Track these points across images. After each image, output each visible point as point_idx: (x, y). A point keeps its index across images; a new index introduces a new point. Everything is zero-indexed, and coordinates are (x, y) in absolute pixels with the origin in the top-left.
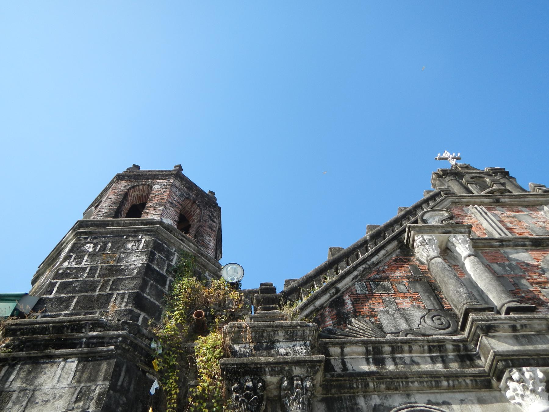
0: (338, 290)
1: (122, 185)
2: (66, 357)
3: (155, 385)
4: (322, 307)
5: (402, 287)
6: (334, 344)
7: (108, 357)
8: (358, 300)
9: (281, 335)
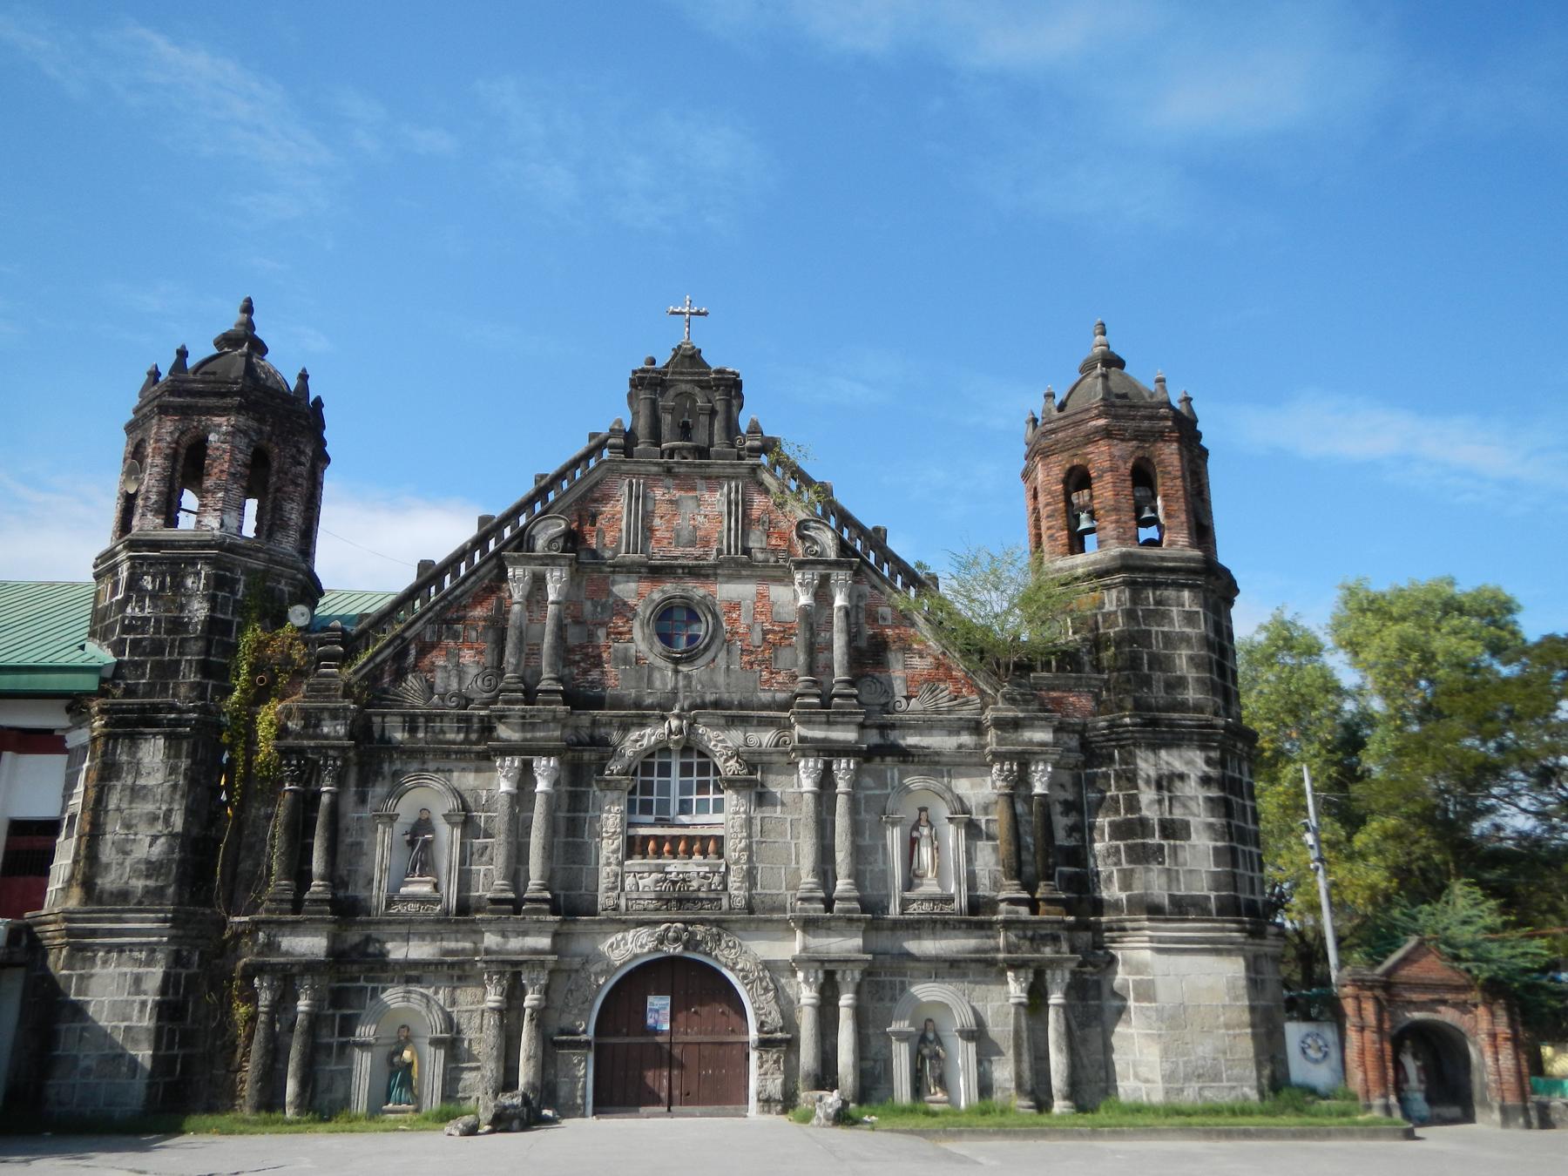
0: (404, 640)
1: (164, 431)
2: (154, 735)
3: (226, 756)
4: (384, 661)
5: (474, 634)
6: (377, 715)
7: (186, 736)
8: (425, 650)
9: (326, 715)
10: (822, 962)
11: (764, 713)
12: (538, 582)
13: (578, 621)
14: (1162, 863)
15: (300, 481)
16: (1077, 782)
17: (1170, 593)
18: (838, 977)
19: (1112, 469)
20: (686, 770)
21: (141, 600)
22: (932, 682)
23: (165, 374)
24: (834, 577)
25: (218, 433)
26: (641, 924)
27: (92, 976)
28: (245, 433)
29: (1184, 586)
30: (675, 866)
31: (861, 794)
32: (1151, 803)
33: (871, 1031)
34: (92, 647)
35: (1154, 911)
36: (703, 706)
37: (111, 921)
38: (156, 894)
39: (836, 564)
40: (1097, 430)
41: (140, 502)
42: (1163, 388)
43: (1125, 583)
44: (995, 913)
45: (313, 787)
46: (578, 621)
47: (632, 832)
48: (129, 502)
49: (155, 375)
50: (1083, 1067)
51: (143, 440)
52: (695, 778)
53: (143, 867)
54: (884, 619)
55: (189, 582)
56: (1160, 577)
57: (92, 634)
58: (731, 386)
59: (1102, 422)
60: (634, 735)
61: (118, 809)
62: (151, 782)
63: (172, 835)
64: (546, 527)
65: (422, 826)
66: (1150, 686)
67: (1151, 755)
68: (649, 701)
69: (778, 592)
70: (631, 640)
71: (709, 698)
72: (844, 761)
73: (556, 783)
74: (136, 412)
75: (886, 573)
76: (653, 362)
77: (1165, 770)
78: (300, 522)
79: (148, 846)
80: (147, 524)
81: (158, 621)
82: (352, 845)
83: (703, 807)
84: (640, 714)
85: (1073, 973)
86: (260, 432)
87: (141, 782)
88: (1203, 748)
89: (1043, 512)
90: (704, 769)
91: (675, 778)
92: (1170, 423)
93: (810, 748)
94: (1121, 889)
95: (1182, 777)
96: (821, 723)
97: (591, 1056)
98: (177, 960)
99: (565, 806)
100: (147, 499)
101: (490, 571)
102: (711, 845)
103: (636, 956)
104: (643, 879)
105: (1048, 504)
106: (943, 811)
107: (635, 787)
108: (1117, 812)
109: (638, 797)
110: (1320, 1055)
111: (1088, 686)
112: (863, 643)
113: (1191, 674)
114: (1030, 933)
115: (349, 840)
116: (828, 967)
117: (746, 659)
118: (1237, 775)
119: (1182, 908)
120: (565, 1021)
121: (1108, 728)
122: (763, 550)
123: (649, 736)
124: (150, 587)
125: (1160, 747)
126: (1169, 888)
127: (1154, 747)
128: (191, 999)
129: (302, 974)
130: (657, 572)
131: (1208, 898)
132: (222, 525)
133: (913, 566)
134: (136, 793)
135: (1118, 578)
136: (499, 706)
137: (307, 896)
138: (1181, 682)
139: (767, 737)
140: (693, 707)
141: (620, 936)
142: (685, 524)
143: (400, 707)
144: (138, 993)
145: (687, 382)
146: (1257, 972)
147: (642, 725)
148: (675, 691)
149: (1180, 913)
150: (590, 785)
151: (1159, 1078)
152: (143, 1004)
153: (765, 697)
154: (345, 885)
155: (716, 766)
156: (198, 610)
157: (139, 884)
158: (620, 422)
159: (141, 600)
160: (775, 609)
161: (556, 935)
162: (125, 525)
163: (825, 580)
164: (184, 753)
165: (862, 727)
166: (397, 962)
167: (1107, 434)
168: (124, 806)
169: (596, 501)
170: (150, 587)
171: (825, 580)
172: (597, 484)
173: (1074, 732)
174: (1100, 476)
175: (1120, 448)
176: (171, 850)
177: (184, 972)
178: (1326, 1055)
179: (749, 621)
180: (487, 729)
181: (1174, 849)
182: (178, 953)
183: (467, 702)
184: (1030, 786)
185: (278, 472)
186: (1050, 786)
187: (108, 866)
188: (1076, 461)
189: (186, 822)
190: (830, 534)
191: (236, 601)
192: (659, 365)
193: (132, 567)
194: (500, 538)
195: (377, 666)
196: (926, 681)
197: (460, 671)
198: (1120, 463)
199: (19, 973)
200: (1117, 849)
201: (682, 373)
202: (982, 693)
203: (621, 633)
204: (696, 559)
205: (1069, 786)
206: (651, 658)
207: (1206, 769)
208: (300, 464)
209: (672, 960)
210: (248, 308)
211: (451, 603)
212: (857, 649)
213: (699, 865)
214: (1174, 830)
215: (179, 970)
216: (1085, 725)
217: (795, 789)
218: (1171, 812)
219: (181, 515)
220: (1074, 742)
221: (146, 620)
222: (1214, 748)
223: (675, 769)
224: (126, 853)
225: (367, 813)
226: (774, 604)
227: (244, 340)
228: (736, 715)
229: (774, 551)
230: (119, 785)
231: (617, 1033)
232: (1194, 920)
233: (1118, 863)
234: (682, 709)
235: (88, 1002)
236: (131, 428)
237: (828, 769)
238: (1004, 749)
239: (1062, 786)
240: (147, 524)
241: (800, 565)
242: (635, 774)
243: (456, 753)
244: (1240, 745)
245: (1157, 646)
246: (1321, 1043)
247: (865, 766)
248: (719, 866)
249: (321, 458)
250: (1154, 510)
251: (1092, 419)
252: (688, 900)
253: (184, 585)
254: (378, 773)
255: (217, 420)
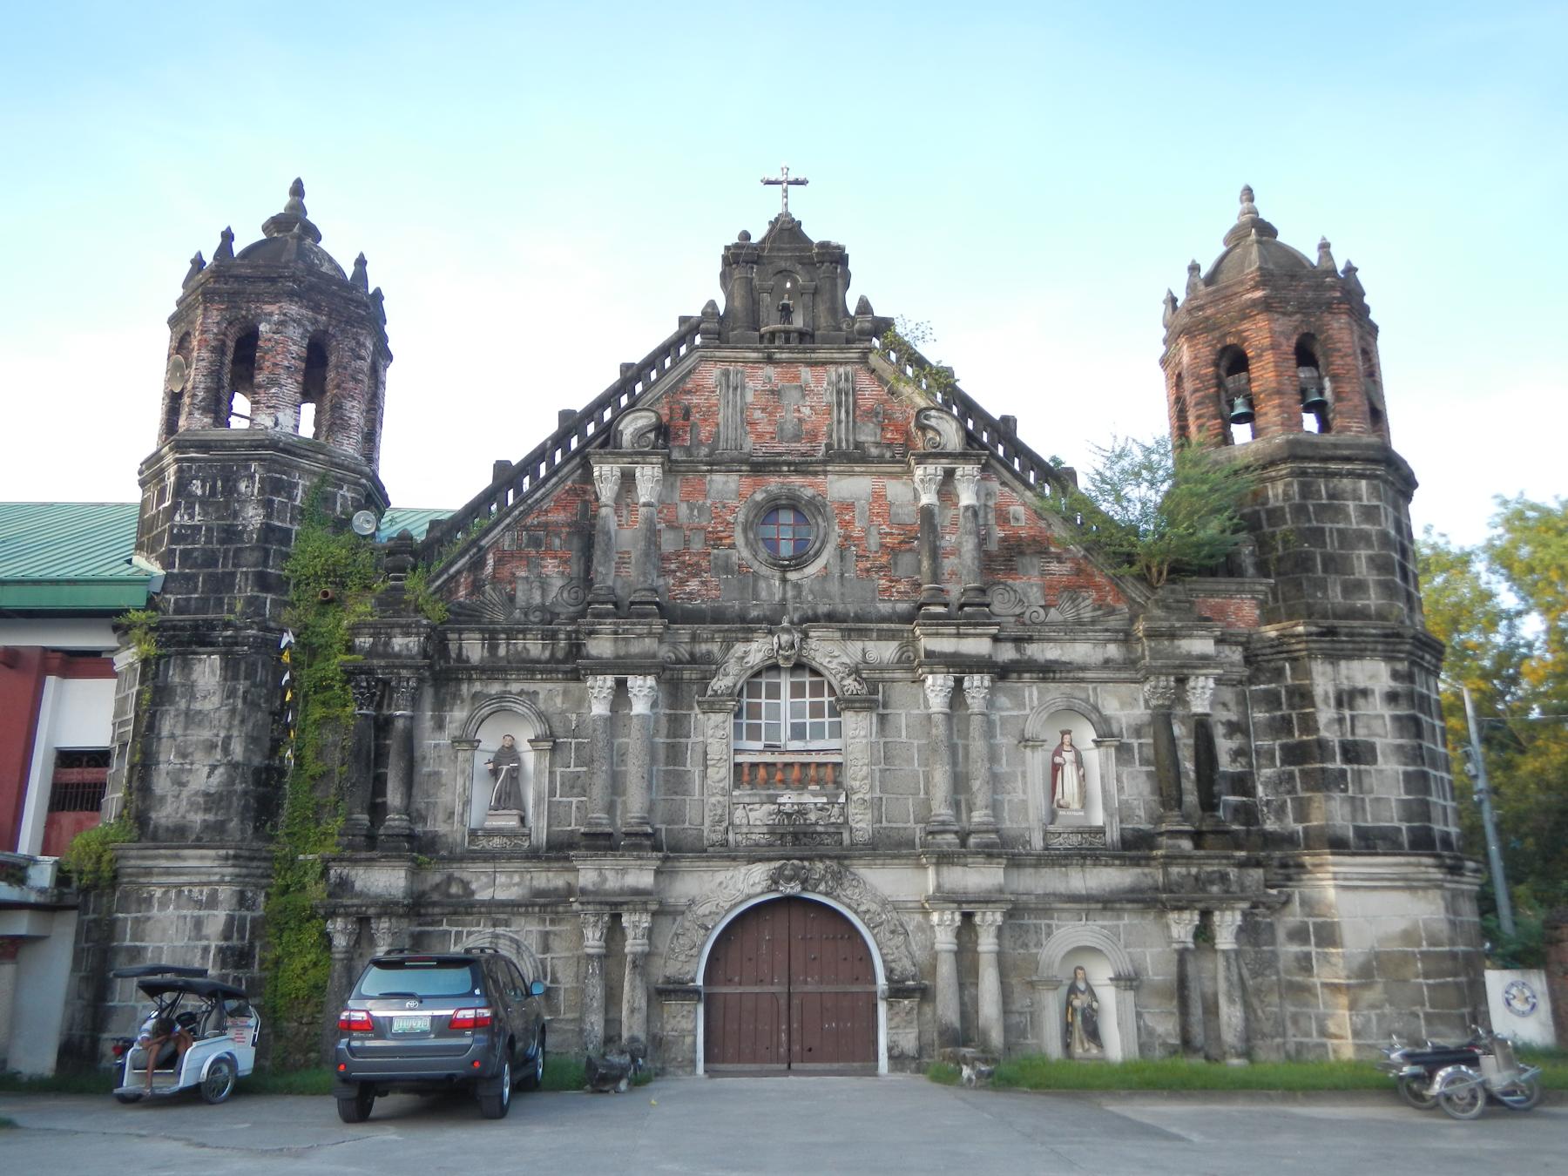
0: (480, 549)
2: (210, 654)
4: (459, 572)
5: (557, 542)
6: (453, 631)
10: (960, 903)
11: (885, 626)
12: (628, 480)
13: (672, 526)
14: (1345, 790)
15: (360, 377)
16: (1242, 701)
17: (1346, 483)
18: (977, 919)
19: (1274, 347)
20: (797, 690)
21: (190, 507)
22: (1072, 591)
23: (209, 259)
24: (959, 473)
25: (269, 322)
26: (753, 860)
27: (149, 919)
28: (299, 322)
29: (1361, 476)
30: (788, 799)
31: (996, 717)
32: (1330, 722)
33: (1014, 981)
34: (140, 561)
35: (1338, 845)
36: (815, 619)
37: (167, 857)
38: (219, 828)
39: (963, 456)
40: (1254, 303)
41: (186, 400)
42: (1329, 255)
43: (1292, 474)
44: (1152, 848)
45: (385, 712)
46: (672, 526)
47: (740, 759)
48: (174, 402)
49: (198, 262)
50: (1257, 1020)
51: (188, 334)
52: (808, 699)
53: (201, 800)
54: (1017, 520)
55: (242, 486)
56: (1333, 466)
57: (139, 547)
58: (834, 259)
59: (1259, 294)
60: (739, 648)
61: (172, 736)
62: (207, 706)
63: (234, 766)
64: (636, 419)
65: (508, 753)
66: (1325, 590)
67: (1329, 668)
68: (754, 613)
69: (895, 490)
70: (732, 546)
71: (823, 609)
72: (977, 677)
73: (654, 705)
74: (179, 303)
75: (1017, 467)
76: (746, 236)
77: (1346, 685)
78: (362, 422)
79: (204, 777)
80: (193, 422)
81: (209, 529)
82: (429, 775)
83: (818, 732)
84: (745, 625)
85: (1245, 915)
86: (315, 322)
87: (197, 706)
88: (1389, 659)
89: (1191, 400)
90: (817, 690)
91: (785, 699)
92: (1338, 294)
93: (936, 660)
94: (1296, 820)
95: (1365, 693)
96: (950, 635)
97: (701, 1009)
98: (242, 900)
99: (664, 730)
100: (194, 396)
101: (573, 472)
102: (830, 775)
103: (750, 897)
104: (755, 816)
105: (1196, 390)
106: (1086, 734)
107: (741, 709)
108: (1290, 733)
109: (745, 721)
110: (1527, 1007)
111: (1252, 592)
112: (993, 547)
113: (1371, 577)
114: (1194, 870)
115: (426, 770)
116: (967, 908)
117: (861, 565)
118: (1425, 691)
119: (1369, 841)
120: (672, 969)
121: (1278, 638)
122: (877, 444)
123: (757, 650)
124: (199, 492)
125: (1339, 658)
126: (1354, 819)
127: (1333, 657)
128: (258, 944)
129: (379, 916)
130: (759, 467)
131: (1399, 830)
132: (276, 424)
133: (1047, 459)
134: (191, 718)
135: (1284, 469)
136: (589, 619)
137: (381, 831)
138: (1359, 587)
139: (885, 651)
140: (805, 619)
141: (730, 874)
142: (789, 417)
143: (479, 622)
144: (199, 937)
145: (786, 259)
146: (1456, 913)
147: (748, 640)
148: (783, 602)
149: (1368, 847)
150: (692, 708)
151: (1349, 1033)
152: (206, 950)
153: (885, 608)
154: (424, 819)
155: (830, 685)
156: (253, 517)
157: (197, 818)
158: (712, 304)
159: (190, 507)
160: (894, 509)
161: (658, 872)
162: (170, 426)
163: (949, 474)
164: (242, 674)
165: (996, 639)
166: (483, 903)
167: (1266, 306)
168: (178, 732)
169: (689, 392)
170: (199, 492)
171: (949, 474)
172: (690, 372)
173: (1237, 643)
174: (1260, 356)
175: (1283, 324)
176: (231, 781)
177: (249, 915)
178: (1534, 1006)
179: (864, 524)
180: (576, 650)
181: (1358, 776)
182: (242, 894)
183: (549, 615)
184: (1186, 704)
185: (337, 367)
186: (1212, 705)
187: (162, 799)
188: (1230, 340)
189: (246, 750)
190: (954, 425)
191: (294, 507)
192: (755, 239)
193: (180, 471)
194: (582, 433)
195: (452, 577)
196: (1066, 588)
197: (544, 586)
198: (1282, 340)
199: (73, 915)
200: (1291, 776)
201: (780, 249)
202: (1131, 601)
203: (721, 539)
204: (803, 455)
205: (1232, 705)
206: (756, 566)
207: (1392, 684)
208: (363, 358)
209: (789, 901)
210: (298, 190)
211: (531, 508)
212: (986, 552)
213: (815, 794)
214: (1357, 752)
215: (244, 913)
216: (1250, 635)
217: (922, 711)
218: (1353, 733)
219: (233, 419)
220: (1236, 654)
221: (197, 528)
222: (1401, 660)
223: (785, 690)
224: (183, 785)
225: (445, 739)
226: (891, 504)
227: (292, 227)
228: (853, 625)
229: (889, 446)
230: (172, 710)
231: (729, 981)
232: (1385, 854)
233: (1292, 791)
234: (792, 622)
235: (145, 948)
236: (174, 321)
237: (959, 682)
238: (1159, 663)
239: (1225, 705)
240: (193, 422)
241: (923, 458)
242: (740, 694)
243: (541, 672)
244: (1428, 657)
245: (1332, 545)
246: (1527, 993)
247: (1000, 684)
248: (837, 796)
249: (383, 355)
250: (1321, 392)
251: (1248, 291)
252: (805, 834)
253: (236, 490)
254: (456, 696)
255: (268, 308)
